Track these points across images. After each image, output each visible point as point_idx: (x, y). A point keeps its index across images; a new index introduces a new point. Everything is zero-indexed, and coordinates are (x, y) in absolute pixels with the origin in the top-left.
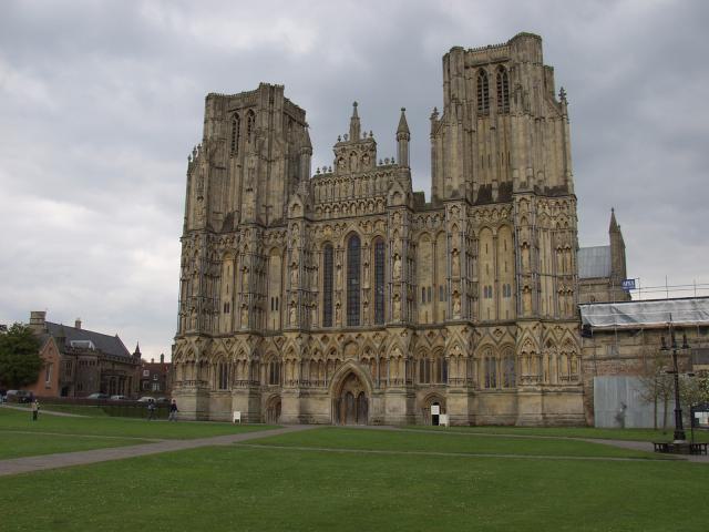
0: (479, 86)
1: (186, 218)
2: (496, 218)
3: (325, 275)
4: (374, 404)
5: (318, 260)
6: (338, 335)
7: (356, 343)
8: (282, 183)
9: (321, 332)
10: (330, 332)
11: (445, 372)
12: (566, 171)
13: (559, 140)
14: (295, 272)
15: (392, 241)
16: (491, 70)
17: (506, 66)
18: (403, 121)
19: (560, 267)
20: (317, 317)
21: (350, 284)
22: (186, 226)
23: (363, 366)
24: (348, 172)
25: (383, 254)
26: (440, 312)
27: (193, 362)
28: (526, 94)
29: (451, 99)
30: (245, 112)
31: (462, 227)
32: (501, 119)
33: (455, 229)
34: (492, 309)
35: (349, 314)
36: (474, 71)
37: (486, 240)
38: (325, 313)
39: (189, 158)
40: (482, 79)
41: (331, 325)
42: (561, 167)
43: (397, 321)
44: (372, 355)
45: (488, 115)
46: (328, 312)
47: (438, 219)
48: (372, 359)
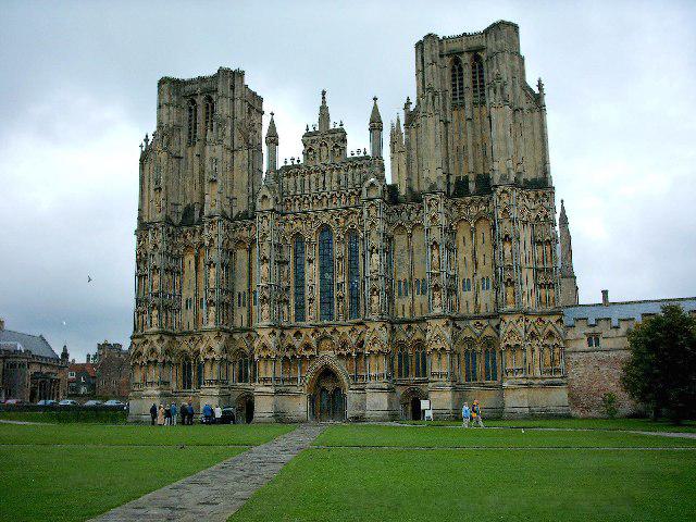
0: (454, 76)
4: (352, 398)
5: (289, 255)
9: (290, 328)
12: (545, 162)
13: (537, 132)
14: (266, 265)
15: (368, 234)
16: (466, 59)
17: (483, 56)
18: (375, 110)
21: (322, 278)
22: (140, 218)
27: (156, 361)
28: (505, 84)
29: (424, 87)
31: (442, 220)
32: (477, 110)
34: (472, 302)
36: (447, 61)
37: (463, 232)
39: (141, 146)
41: (303, 319)
42: (539, 159)
44: (349, 351)
45: (463, 106)
46: (300, 307)
48: (349, 355)
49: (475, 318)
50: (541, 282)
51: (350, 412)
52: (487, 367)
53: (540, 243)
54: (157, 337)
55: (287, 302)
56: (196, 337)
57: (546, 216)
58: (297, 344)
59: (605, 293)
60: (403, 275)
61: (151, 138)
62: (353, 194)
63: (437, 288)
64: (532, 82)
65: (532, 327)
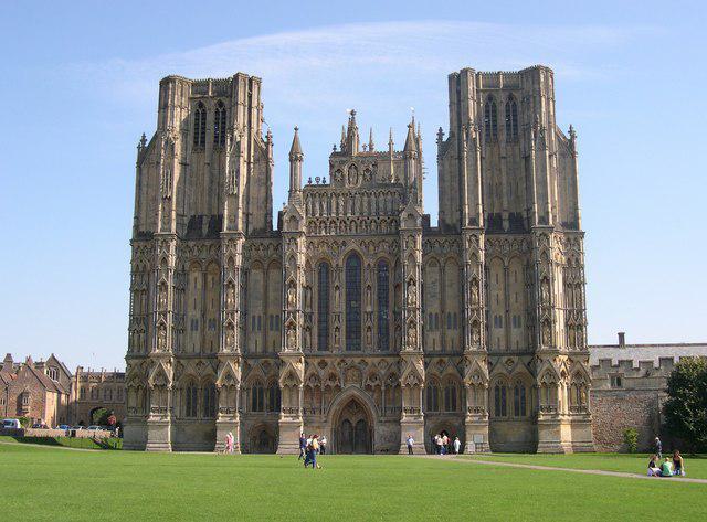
3: (319, 294)
6: (339, 360)
7: (359, 369)
8: (263, 189)
10: (329, 356)
11: (454, 401)
12: (576, 208)
16: (502, 98)
22: (136, 227)
25: (387, 277)
26: (448, 339)
30: (213, 102)
35: (348, 337)
38: (320, 336)
40: (491, 104)
41: (327, 348)
43: (409, 349)
44: (377, 382)
45: (496, 141)
49: (507, 355)
51: (378, 442)
52: (516, 403)
56: (204, 361)
57: (577, 260)
58: (322, 373)
59: (621, 336)
61: (149, 138)
64: (563, 125)
65: (563, 367)
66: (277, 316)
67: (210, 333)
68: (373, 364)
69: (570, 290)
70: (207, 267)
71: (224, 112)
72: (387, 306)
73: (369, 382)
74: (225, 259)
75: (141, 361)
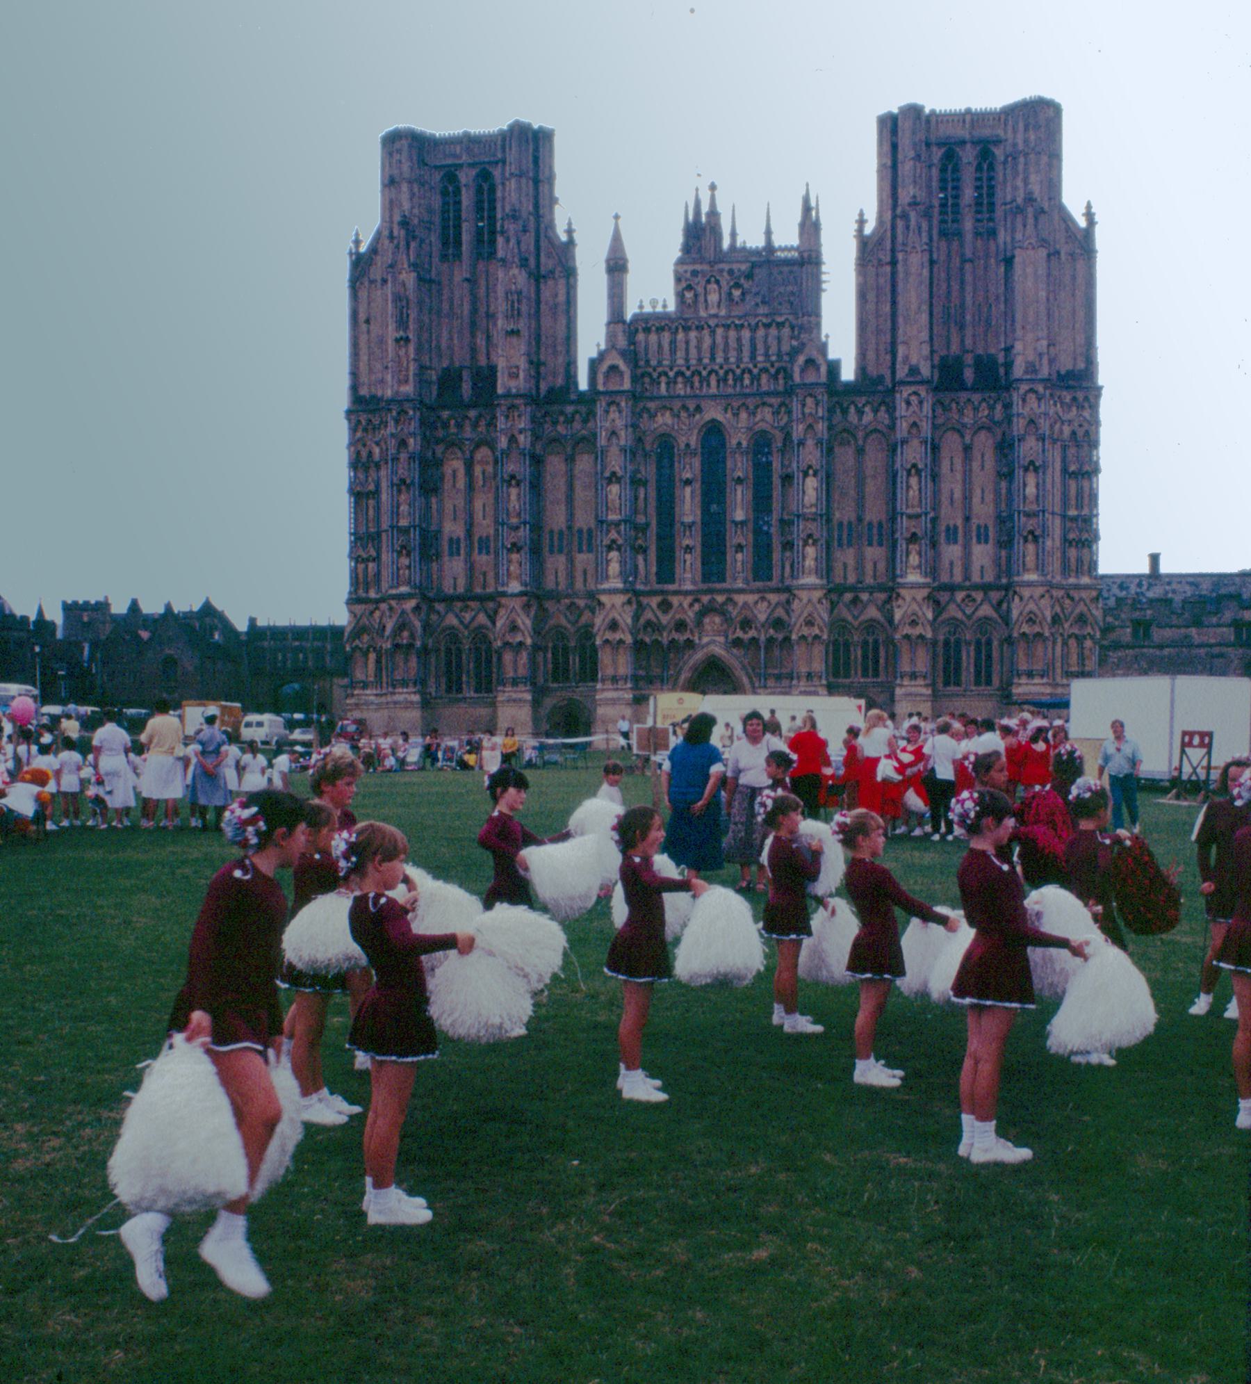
1: (354, 374)
2: (969, 412)
5: (649, 471)
6: (689, 599)
14: (615, 489)
19: (1073, 502)
20: (647, 565)
22: (354, 388)
23: (735, 651)
24: (703, 314)
25: (770, 464)
27: (411, 646)
30: (474, 172)
31: (926, 428)
33: (914, 431)
39: (351, 254)
41: (672, 580)
43: (811, 580)
44: (752, 633)
47: (867, 409)
48: (754, 640)
50: (1071, 536)
53: (1074, 475)
54: (412, 603)
55: (644, 550)
57: (1087, 433)
58: (665, 619)
60: (844, 513)
62: (764, 370)
63: (913, 538)
65: (1058, 609)
66: (590, 530)
67: (482, 559)
68: (746, 603)
69: (1073, 485)
70: (472, 452)
71: (492, 189)
72: (769, 512)
73: (739, 634)
74: (503, 442)
75: (372, 607)
